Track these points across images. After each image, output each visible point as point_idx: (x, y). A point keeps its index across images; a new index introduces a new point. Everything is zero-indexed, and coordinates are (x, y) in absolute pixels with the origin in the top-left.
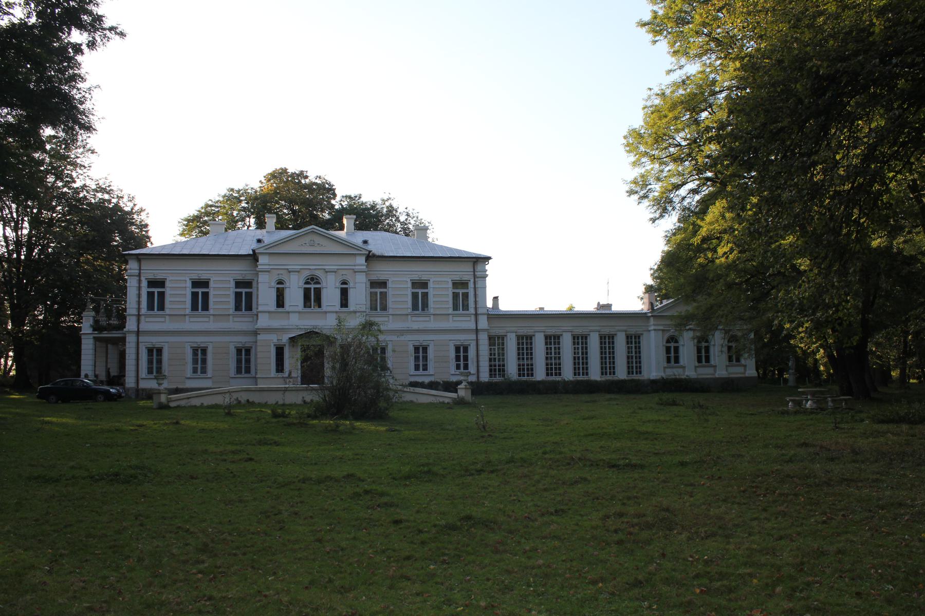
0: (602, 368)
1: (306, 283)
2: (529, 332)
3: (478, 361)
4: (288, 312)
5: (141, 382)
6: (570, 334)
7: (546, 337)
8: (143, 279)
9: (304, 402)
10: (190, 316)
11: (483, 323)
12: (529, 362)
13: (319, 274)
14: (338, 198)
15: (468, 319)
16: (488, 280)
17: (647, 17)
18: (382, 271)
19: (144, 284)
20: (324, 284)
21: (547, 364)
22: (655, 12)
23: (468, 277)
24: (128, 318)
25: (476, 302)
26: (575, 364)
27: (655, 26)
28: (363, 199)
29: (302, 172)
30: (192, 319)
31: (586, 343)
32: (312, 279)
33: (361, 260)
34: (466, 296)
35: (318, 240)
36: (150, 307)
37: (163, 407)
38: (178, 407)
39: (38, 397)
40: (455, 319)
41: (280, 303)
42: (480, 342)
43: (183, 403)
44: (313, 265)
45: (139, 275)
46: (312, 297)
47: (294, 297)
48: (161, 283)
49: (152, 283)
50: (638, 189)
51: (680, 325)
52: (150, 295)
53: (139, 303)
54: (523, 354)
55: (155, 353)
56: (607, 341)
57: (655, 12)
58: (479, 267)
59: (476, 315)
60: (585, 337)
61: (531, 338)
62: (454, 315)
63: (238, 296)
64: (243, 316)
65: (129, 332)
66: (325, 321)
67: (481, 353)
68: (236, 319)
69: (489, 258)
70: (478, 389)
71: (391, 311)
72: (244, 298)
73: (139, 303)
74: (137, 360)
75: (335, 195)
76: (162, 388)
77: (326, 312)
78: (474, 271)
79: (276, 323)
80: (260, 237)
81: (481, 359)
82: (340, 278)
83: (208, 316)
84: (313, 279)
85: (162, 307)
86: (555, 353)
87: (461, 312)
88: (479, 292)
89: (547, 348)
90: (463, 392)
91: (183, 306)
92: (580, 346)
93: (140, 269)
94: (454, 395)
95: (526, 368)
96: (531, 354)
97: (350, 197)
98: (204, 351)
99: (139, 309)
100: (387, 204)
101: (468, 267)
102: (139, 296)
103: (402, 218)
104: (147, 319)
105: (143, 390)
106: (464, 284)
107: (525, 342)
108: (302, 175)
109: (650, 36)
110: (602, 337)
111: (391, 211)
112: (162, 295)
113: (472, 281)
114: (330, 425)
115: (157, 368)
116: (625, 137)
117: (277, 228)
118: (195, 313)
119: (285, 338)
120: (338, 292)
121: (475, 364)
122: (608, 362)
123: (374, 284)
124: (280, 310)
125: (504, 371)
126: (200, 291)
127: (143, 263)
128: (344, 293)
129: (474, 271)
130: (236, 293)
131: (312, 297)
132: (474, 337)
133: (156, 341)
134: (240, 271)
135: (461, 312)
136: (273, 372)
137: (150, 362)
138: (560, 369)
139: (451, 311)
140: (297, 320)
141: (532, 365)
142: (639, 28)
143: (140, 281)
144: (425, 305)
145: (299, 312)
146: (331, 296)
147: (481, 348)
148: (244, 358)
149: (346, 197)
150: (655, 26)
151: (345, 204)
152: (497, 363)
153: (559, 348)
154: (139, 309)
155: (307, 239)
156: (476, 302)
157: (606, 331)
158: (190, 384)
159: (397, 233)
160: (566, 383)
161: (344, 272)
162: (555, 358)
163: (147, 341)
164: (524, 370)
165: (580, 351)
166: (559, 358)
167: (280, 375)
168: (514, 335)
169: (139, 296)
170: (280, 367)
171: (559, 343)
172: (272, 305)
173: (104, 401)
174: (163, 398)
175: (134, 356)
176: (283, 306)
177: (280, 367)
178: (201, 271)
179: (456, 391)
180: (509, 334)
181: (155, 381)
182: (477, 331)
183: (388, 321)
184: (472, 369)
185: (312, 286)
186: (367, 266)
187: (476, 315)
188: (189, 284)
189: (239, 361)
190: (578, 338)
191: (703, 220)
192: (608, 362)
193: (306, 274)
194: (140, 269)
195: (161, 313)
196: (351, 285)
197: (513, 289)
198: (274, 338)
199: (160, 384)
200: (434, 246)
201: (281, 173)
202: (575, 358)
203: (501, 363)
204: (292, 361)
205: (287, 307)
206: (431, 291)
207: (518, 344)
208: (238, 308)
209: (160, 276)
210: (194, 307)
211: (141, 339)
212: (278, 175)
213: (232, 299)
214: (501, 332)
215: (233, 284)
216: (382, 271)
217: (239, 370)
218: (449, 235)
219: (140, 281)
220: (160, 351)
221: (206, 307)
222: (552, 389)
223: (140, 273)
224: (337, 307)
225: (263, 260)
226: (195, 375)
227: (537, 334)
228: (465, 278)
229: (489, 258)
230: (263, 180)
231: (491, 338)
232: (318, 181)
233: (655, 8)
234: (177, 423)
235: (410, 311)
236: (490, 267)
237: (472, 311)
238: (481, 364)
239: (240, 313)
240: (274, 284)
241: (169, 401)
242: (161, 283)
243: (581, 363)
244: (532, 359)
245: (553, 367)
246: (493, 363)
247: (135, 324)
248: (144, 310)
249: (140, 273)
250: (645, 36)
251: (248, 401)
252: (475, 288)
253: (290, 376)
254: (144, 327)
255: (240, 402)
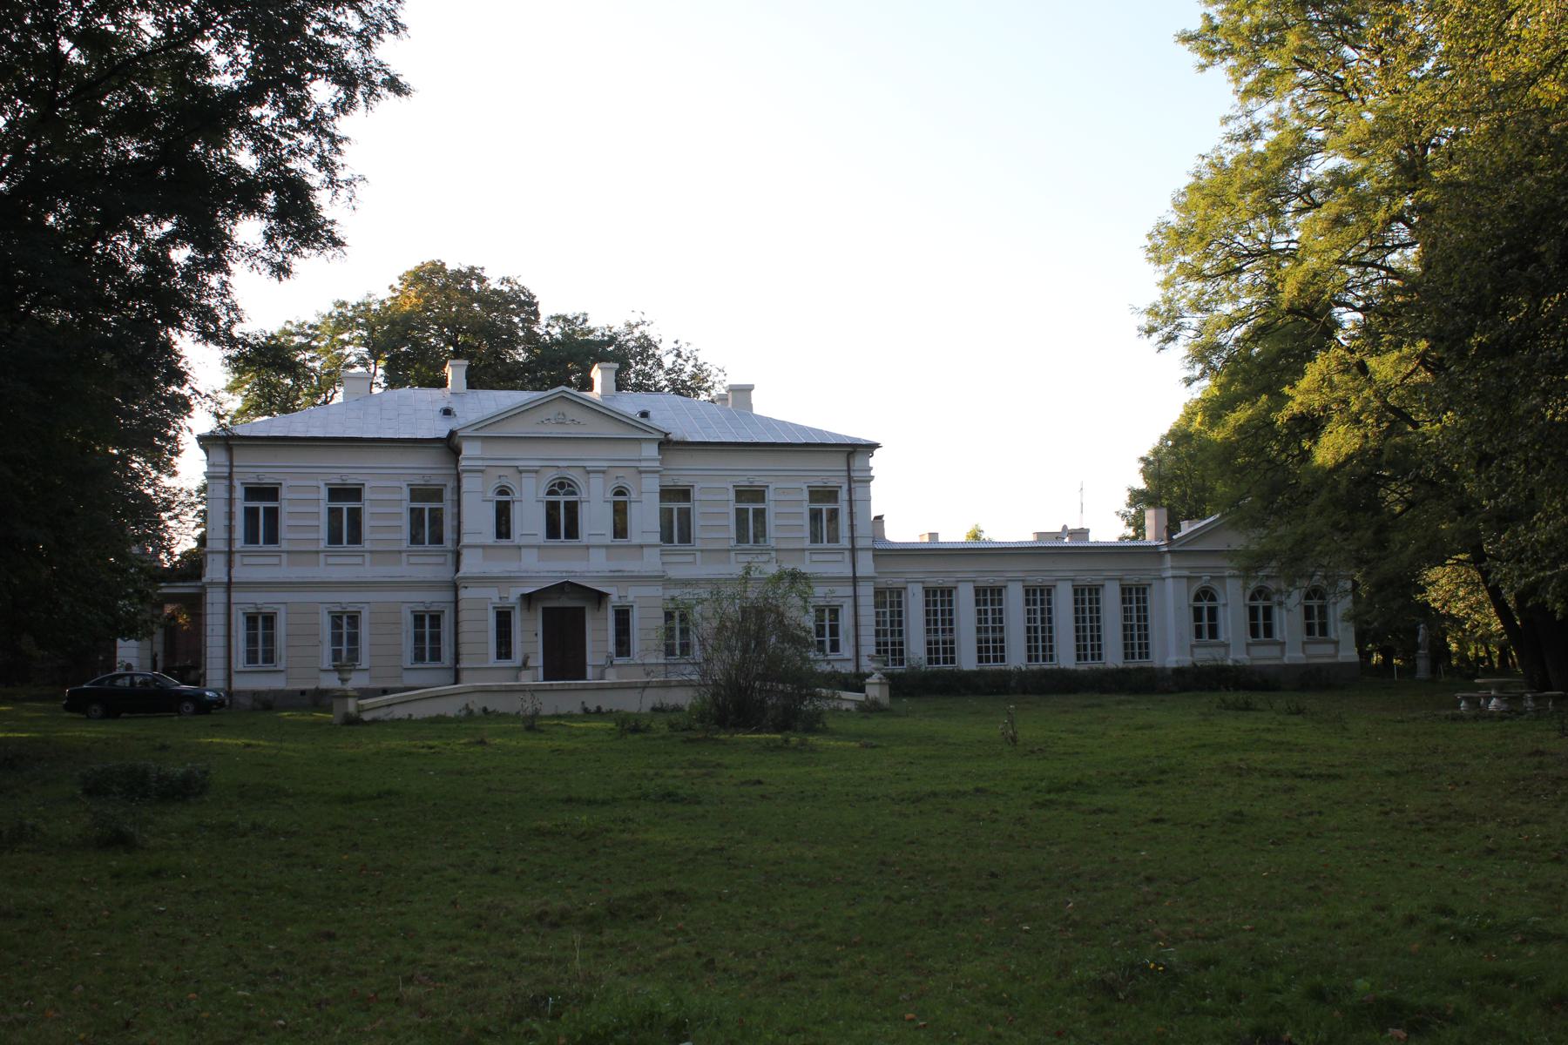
0: (1126, 646)
1: (550, 493)
2: (948, 582)
3: (857, 636)
4: (520, 547)
5: (235, 678)
6: (1020, 585)
7: (977, 591)
8: (237, 483)
9: (586, 711)
10: (328, 554)
11: (866, 566)
12: (948, 638)
13: (573, 475)
14: (543, 321)
15: (839, 557)
16: (875, 488)
17: (1195, 25)
18: (685, 470)
19: (239, 493)
20: (583, 495)
21: (979, 641)
22: (1208, 18)
23: (837, 479)
24: (209, 557)
25: (852, 526)
26: (1029, 640)
27: (1208, 43)
28: (591, 324)
29: (472, 269)
30: (331, 560)
31: (1049, 603)
32: (561, 485)
33: (651, 451)
34: (834, 514)
35: (572, 412)
36: (251, 537)
37: (352, 721)
38: (374, 721)
39: (67, 708)
40: (815, 557)
41: (503, 527)
42: (861, 601)
43: (380, 714)
44: (565, 459)
45: (230, 477)
46: (562, 521)
47: (529, 518)
48: (271, 493)
49: (253, 492)
50: (1158, 323)
51: (1247, 569)
52: (251, 514)
53: (230, 529)
54: (936, 622)
55: (261, 624)
56: (1087, 597)
57: (1208, 18)
58: (857, 463)
59: (853, 550)
60: (1047, 591)
61: (950, 593)
62: (813, 552)
63: (416, 515)
64: (425, 553)
65: (212, 584)
66: (586, 563)
67: (862, 620)
68: (413, 560)
69: (876, 446)
70: (901, 686)
71: (699, 545)
72: (430, 521)
73: (230, 529)
74: (229, 636)
75: (536, 314)
76: (349, 686)
77: (588, 547)
78: (849, 470)
79: (496, 568)
80: (445, 405)
81: (862, 631)
82: (613, 484)
83: (361, 554)
84: (562, 485)
85: (272, 538)
86: (994, 621)
87: (825, 545)
88: (857, 509)
89: (979, 612)
90: (875, 690)
91: (314, 536)
92: (1038, 607)
93: (231, 466)
94: (859, 696)
95: (942, 648)
96: (951, 622)
97: (565, 319)
98: (354, 619)
99: (230, 541)
100: (637, 333)
101: (839, 463)
102: (230, 516)
103: (668, 362)
104: (246, 560)
105: (239, 692)
106: (830, 494)
107: (939, 600)
108: (472, 273)
109: (1198, 58)
110: (1078, 591)
111: (646, 347)
112: (272, 515)
113: (845, 487)
114: (774, 740)
115: (265, 652)
116: (1150, 236)
117: (471, 385)
118: (336, 548)
119: (513, 595)
120: (609, 509)
121: (852, 640)
122: (1089, 639)
123: (667, 494)
124: (504, 542)
125: (901, 652)
126: (345, 506)
127: (236, 452)
128: (620, 511)
129: (849, 470)
130: (412, 510)
131: (562, 521)
132: (849, 591)
133: (262, 600)
134: (425, 469)
135: (825, 545)
136: (492, 660)
137: (251, 640)
138: (1002, 649)
139: (807, 544)
140: (542, 564)
141: (952, 642)
142: (1180, 45)
143: (231, 488)
144: (761, 533)
145: (539, 547)
146: (595, 518)
147: (861, 611)
148: (431, 633)
149: (557, 318)
150: (1208, 43)
151: (556, 332)
152: (990, 635)
153: (1001, 611)
154: (230, 541)
155: (551, 412)
156: (852, 526)
157: (1087, 579)
158: (410, 679)
159: (659, 390)
160: (1063, 673)
161: (620, 473)
162: (994, 629)
163: (245, 601)
164: (937, 650)
165: (1039, 616)
166: (1002, 629)
167: (505, 663)
168: (920, 586)
169: (230, 516)
170: (504, 650)
171: (1000, 603)
172: (489, 536)
173: (102, 717)
174: (351, 706)
175: (221, 630)
176: (508, 536)
177: (504, 650)
178: (346, 468)
179: (861, 689)
180: (910, 586)
181: (336, 675)
182: (855, 580)
183: (694, 563)
184: (846, 650)
185: (562, 499)
186: (661, 461)
187: (853, 550)
188: (324, 494)
189: (419, 638)
190: (1035, 592)
191: (1293, 386)
192: (1089, 639)
193: (550, 476)
194: (231, 466)
195: (272, 547)
196: (634, 496)
197: (912, 504)
198: (493, 595)
199: (344, 681)
200: (768, 423)
201: (431, 272)
202: (1029, 629)
203: (897, 639)
204: (529, 637)
205: (516, 538)
206: (771, 507)
207: (927, 604)
208: (415, 539)
209: (268, 479)
210: (334, 538)
211: (235, 597)
212: (428, 277)
213: (405, 522)
214: (896, 582)
215: (406, 494)
216: (685, 470)
217: (419, 657)
218: (792, 401)
219: (231, 488)
220: (270, 620)
221: (356, 538)
222: (991, 686)
223: (231, 473)
224: (608, 538)
225: (469, 450)
226: (252, 667)
227: (961, 586)
228: (833, 483)
229: (876, 446)
230: (397, 285)
231: (879, 593)
232: (506, 289)
233: (1212, 11)
234: (482, 742)
235: (733, 543)
236: (876, 461)
237: (845, 543)
238: (863, 640)
239: (420, 548)
240: (491, 494)
241: (361, 709)
242: (271, 493)
243: (1040, 637)
244: (951, 630)
245: (991, 647)
246: (882, 639)
247: (225, 570)
248: (239, 544)
249: (231, 473)
250: (1190, 57)
251: (485, 710)
252: (850, 501)
253: (525, 665)
254: (240, 574)
255: (471, 712)
